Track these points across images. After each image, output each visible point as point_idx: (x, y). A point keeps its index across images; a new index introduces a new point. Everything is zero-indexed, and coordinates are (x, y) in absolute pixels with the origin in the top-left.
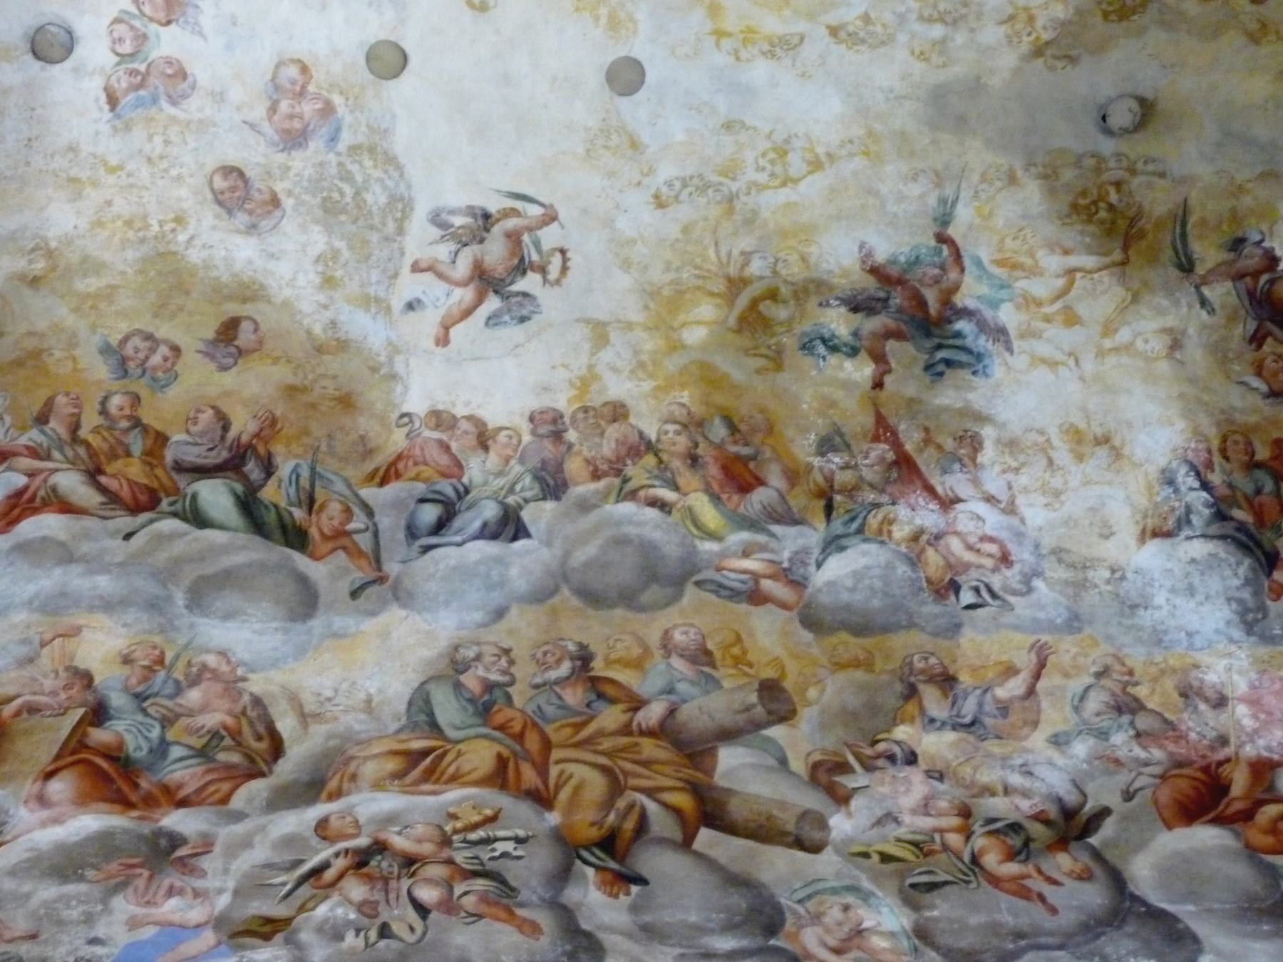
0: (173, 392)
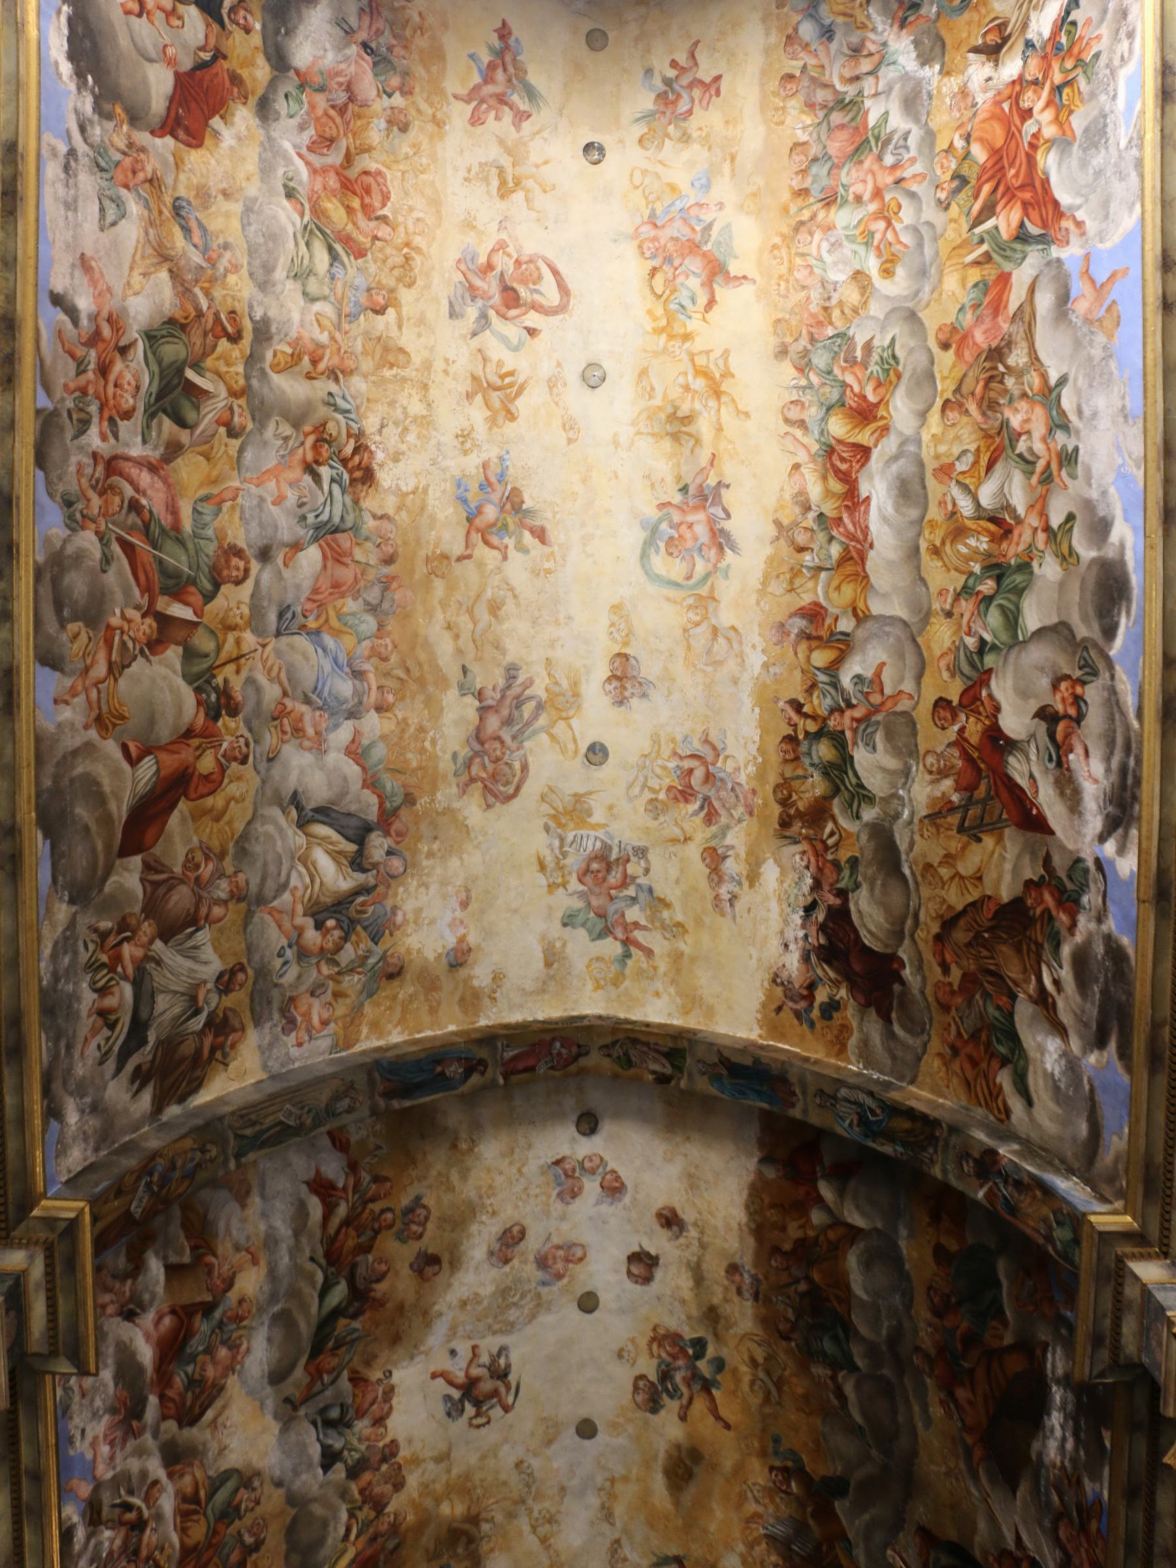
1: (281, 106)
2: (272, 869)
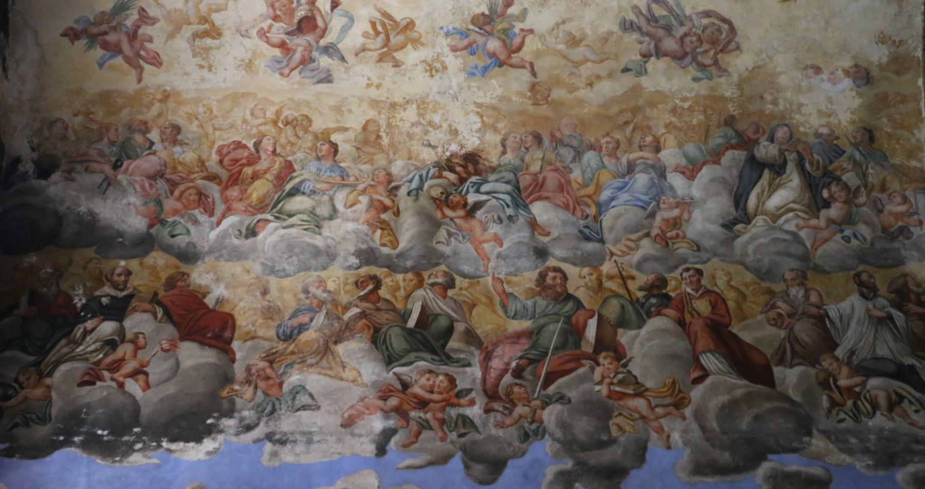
1: (181, 241)
2: (782, 247)
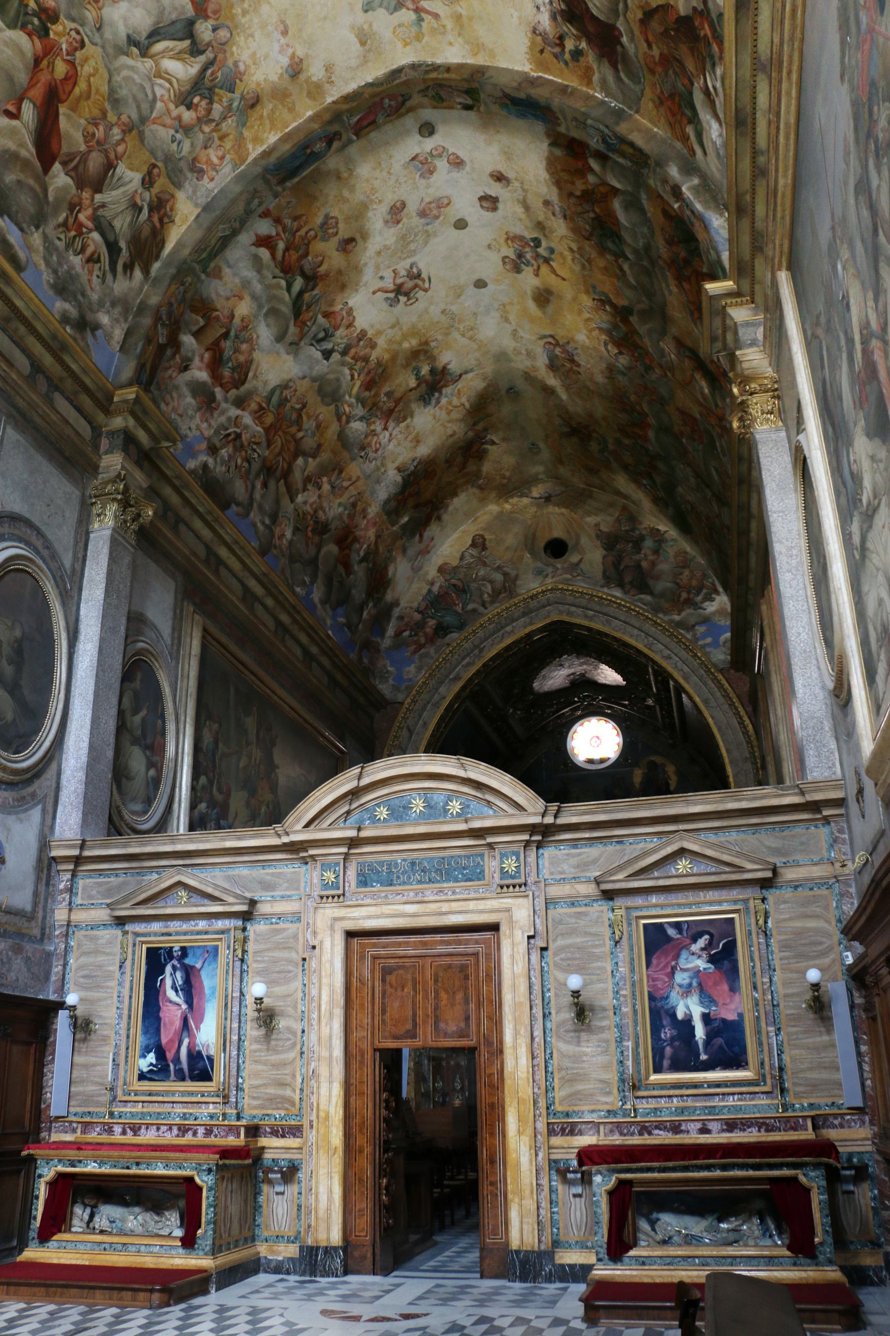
0: (323, 244)
2: (140, 96)
